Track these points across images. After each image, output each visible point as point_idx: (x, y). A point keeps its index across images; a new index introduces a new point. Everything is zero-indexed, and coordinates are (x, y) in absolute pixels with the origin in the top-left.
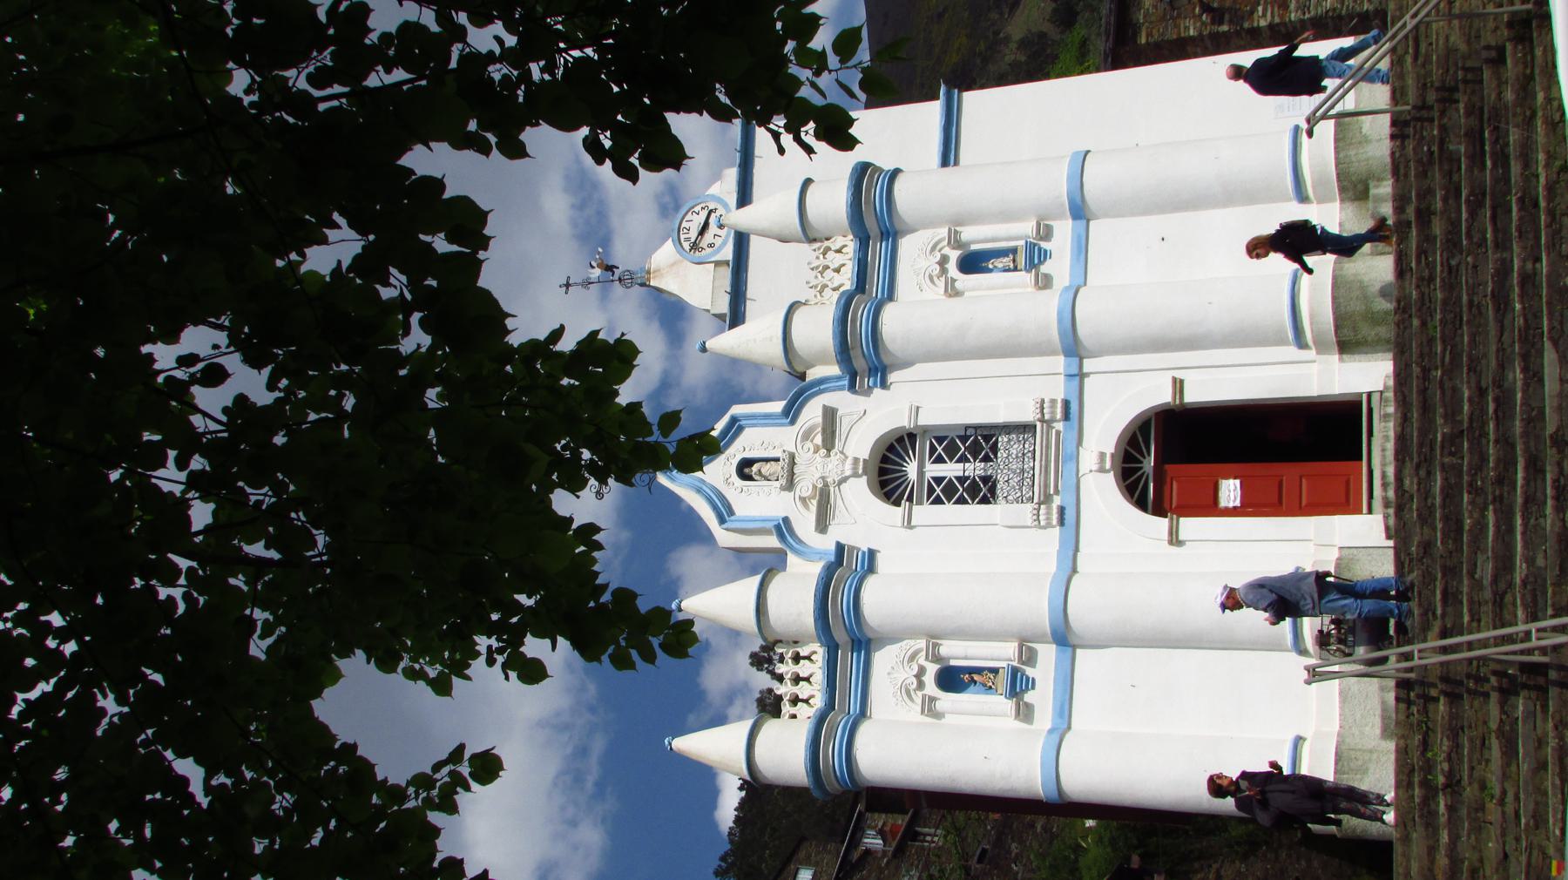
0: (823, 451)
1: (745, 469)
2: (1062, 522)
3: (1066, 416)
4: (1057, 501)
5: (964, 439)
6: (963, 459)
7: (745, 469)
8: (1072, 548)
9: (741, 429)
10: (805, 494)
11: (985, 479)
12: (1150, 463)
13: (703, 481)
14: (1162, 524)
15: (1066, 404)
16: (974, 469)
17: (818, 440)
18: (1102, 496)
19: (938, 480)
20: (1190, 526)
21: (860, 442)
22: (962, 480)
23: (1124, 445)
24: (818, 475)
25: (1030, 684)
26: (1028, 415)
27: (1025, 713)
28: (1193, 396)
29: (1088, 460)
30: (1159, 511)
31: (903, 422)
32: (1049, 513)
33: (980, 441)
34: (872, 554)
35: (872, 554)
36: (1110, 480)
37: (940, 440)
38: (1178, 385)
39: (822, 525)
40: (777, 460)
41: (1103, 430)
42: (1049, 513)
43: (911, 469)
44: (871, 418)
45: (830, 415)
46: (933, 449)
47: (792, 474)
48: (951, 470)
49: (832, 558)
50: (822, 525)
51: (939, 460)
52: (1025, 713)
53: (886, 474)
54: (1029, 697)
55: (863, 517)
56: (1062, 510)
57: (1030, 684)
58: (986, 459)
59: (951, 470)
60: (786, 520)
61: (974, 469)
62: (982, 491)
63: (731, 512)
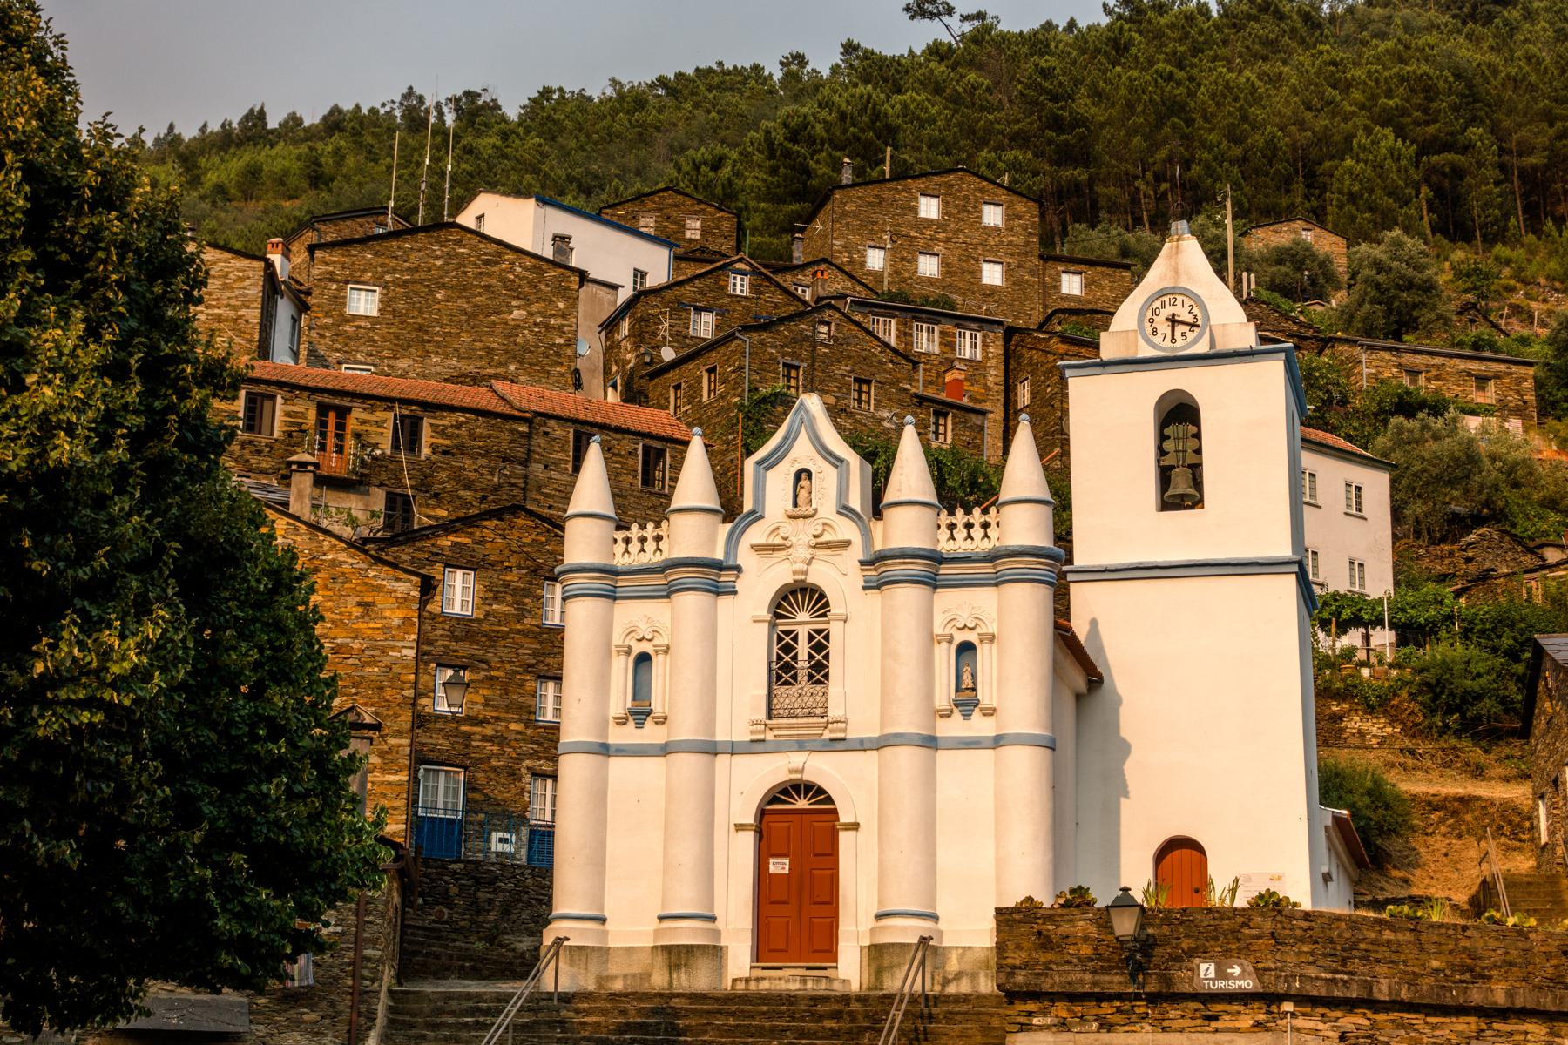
0: (814, 542)
1: (802, 475)
3: (832, 740)
4: (770, 736)
6: (811, 657)
7: (802, 475)
8: (734, 749)
10: (782, 533)
11: (795, 677)
12: (802, 804)
16: (803, 663)
17: (826, 538)
18: (772, 770)
19: (795, 639)
21: (822, 574)
22: (795, 658)
25: (640, 724)
26: (834, 713)
27: (621, 722)
30: (762, 814)
31: (835, 609)
32: (759, 732)
33: (819, 671)
34: (735, 593)
35: (735, 593)
37: (827, 638)
41: (820, 768)
42: (759, 732)
43: (803, 616)
47: (796, 517)
48: (803, 649)
51: (811, 638)
52: (621, 722)
55: (761, 581)
58: (810, 677)
59: (803, 649)
60: (761, 517)
61: (803, 663)
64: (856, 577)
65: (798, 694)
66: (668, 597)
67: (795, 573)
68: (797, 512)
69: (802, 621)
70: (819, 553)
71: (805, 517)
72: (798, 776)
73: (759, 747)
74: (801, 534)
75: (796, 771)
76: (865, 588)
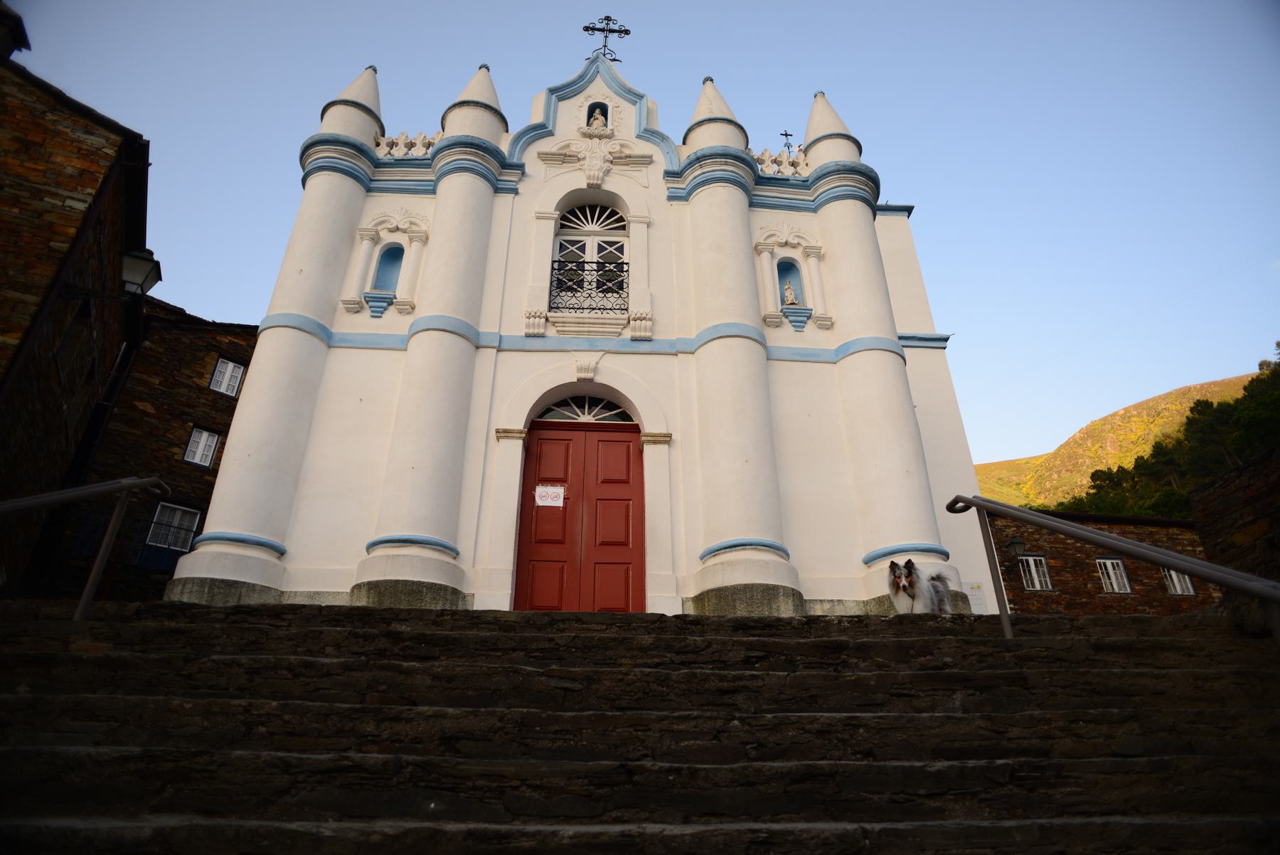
1: (598, 109)
2: (528, 336)
3: (634, 340)
4: (551, 332)
5: (620, 266)
6: (601, 266)
7: (598, 109)
9: (634, 103)
13: (591, 81)
14: (519, 423)
15: (648, 340)
16: (590, 276)
20: (515, 449)
22: (581, 265)
23: (608, 397)
24: (588, 154)
26: (635, 309)
28: (649, 452)
29: (589, 359)
36: (572, 377)
37: (621, 249)
38: (666, 439)
39: (545, 157)
40: (606, 125)
43: (592, 227)
44: (638, 191)
45: (647, 161)
46: (611, 244)
47: (591, 136)
49: (509, 161)
50: (545, 157)
51: (601, 249)
53: (589, 206)
54: (367, 313)
55: (546, 188)
56: (542, 336)
57: (378, 313)
58: (600, 285)
61: (590, 276)
62: (566, 277)
63: (561, 99)
64: (661, 187)
65: (589, 296)
66: (433, 192)
67: (589, 178)
68: (593, 130)
69: (592, 235)
70: (615, 168)
71: (600, 137)
72: (590, 375)
73: (537, 343)
74: (595, 154)
75: (587, 370)
76: (671, 198)
